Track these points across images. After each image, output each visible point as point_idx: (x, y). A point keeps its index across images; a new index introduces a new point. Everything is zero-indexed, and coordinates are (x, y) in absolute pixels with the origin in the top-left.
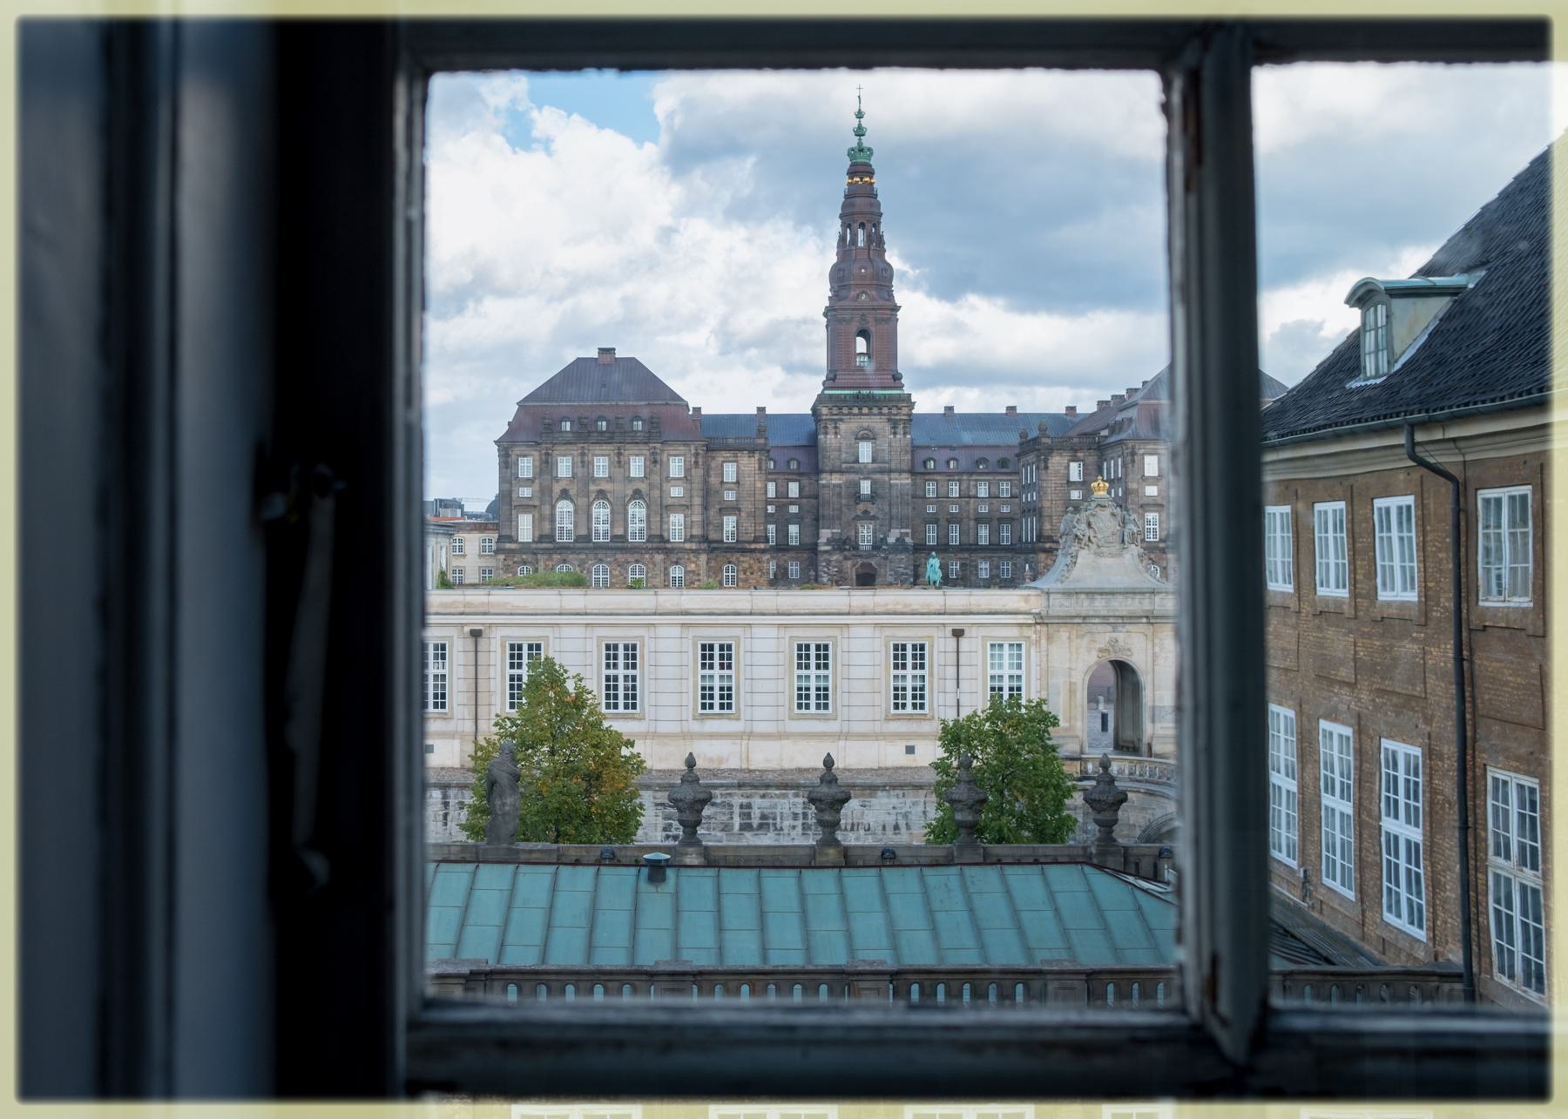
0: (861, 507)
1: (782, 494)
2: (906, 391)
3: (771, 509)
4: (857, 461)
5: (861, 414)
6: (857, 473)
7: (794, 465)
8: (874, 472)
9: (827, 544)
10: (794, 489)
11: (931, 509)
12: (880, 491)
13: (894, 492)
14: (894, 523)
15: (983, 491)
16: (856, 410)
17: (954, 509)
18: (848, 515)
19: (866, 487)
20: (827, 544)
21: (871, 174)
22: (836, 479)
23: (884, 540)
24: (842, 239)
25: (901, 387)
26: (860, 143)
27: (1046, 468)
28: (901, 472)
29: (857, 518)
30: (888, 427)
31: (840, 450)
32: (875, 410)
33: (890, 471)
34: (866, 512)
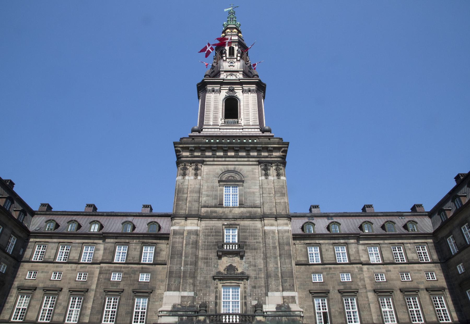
1: (134, 263)
3: (115, 277)
4: (220, 205)
6: (219, 218)
8: (242, 218)
11: (318, 278)
12: (251, 241)
13: (270, 241)
14: (273, 283)
17: (346, 278)
18: (205, 272)
19: (231, 236)
22: (192, 225)
23: (258, 308)
29: (219, 277)
30: (258, 170)
31: (199, 192)
33: (263, 217)
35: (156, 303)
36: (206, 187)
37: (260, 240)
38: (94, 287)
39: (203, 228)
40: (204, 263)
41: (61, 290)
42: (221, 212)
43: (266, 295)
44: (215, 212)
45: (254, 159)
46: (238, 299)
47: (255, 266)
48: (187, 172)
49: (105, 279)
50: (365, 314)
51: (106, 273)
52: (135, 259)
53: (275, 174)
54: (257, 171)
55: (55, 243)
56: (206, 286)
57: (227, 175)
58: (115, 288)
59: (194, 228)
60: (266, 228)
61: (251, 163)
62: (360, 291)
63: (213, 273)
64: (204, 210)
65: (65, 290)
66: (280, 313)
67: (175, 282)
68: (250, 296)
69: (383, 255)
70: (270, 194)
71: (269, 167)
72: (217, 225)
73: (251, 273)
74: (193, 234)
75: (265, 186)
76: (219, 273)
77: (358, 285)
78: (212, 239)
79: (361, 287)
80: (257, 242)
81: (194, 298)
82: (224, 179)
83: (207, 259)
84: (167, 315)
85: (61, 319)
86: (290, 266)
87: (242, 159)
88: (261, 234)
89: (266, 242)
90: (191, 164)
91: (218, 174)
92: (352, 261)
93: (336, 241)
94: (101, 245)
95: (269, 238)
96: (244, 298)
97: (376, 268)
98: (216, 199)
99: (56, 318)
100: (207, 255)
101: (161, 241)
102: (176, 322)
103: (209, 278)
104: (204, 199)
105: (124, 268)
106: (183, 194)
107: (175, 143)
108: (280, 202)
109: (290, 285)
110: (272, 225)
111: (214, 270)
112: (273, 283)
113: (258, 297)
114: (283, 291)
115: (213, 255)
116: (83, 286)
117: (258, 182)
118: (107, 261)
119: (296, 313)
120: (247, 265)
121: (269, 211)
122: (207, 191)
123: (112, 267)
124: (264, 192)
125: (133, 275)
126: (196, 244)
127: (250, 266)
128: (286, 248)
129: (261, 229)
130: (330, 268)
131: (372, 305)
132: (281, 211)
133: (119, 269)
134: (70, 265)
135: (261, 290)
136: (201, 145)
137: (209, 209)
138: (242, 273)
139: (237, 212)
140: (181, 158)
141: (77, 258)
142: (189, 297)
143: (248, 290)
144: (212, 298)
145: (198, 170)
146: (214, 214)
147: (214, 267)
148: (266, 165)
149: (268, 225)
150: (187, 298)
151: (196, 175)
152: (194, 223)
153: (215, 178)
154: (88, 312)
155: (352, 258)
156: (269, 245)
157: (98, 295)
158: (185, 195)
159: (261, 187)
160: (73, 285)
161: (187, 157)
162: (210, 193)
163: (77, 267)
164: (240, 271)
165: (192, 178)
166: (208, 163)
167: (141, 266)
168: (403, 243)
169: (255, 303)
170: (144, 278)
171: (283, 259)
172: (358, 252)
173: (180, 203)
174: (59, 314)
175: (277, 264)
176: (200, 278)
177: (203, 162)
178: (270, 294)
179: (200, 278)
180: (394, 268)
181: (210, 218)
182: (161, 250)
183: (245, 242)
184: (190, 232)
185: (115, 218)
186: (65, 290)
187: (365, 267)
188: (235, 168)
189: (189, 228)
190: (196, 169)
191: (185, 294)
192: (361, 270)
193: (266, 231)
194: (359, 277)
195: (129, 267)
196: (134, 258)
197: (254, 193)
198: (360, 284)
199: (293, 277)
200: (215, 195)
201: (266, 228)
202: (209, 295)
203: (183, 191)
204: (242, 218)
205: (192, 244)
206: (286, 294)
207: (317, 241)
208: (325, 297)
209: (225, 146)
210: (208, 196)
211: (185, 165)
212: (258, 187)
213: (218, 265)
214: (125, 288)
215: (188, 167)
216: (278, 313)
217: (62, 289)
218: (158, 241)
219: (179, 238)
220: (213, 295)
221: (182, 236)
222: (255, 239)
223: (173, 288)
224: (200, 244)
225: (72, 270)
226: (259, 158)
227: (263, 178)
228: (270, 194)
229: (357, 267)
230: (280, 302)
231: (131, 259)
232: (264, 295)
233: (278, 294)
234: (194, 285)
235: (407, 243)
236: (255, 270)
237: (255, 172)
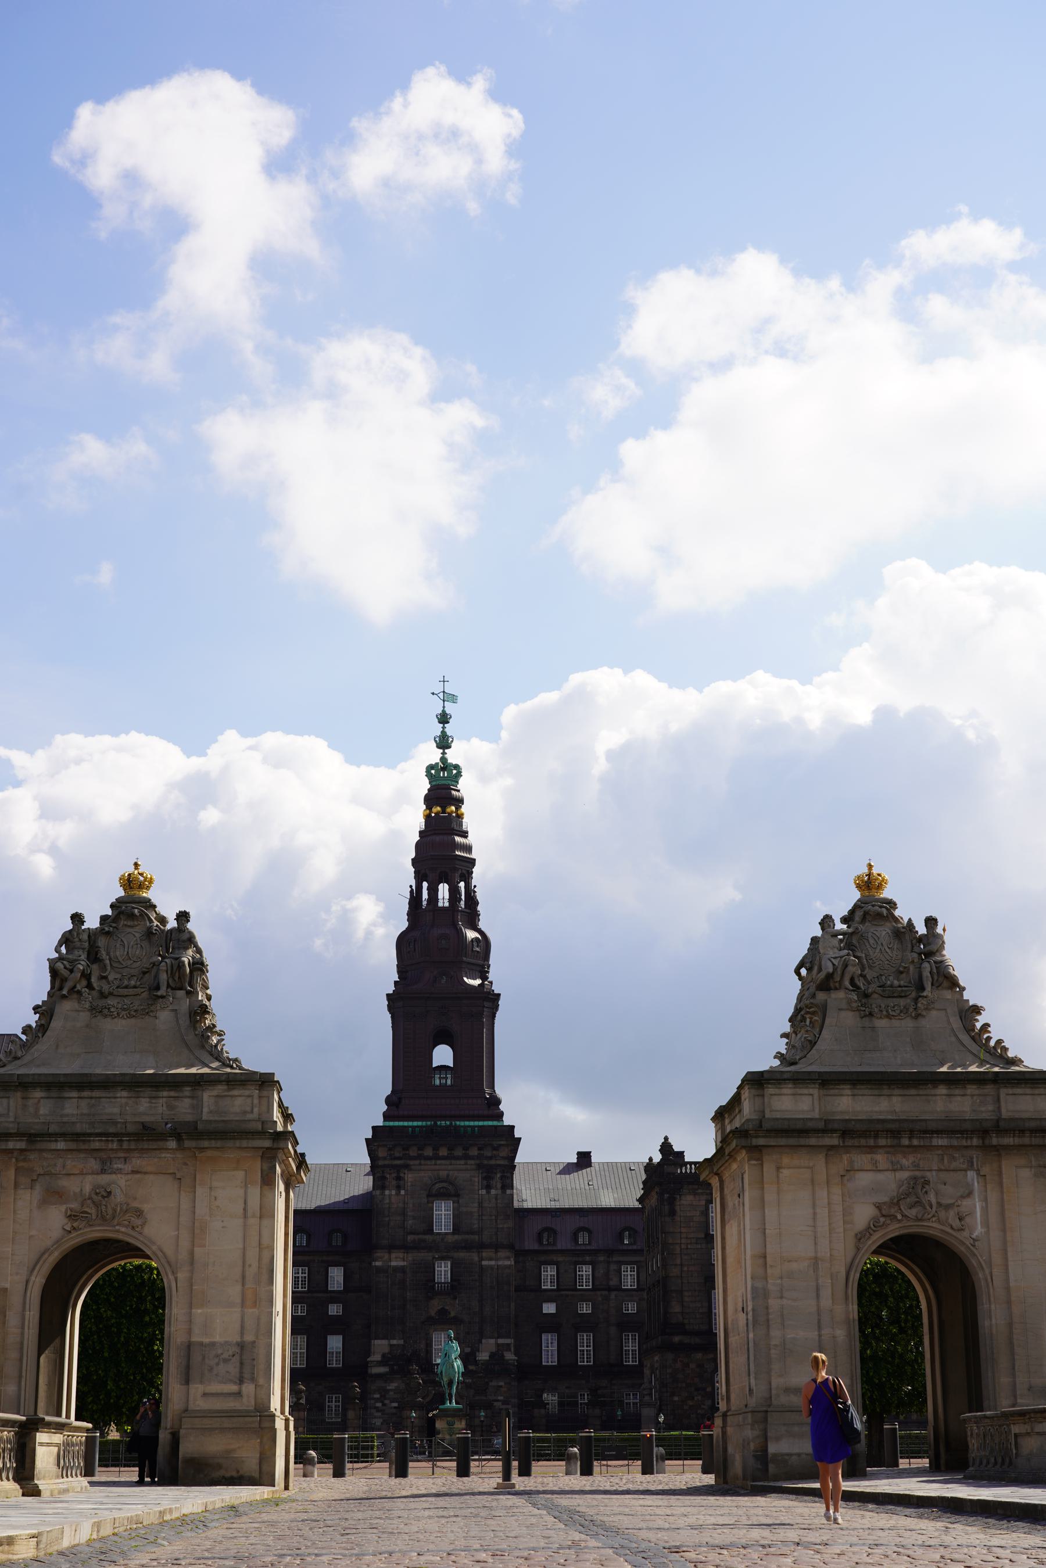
0: (436, 1305)
2: (507, 1121)
4: (430, 1230)
5: (436, 1157)
7: (337, 1240)
8: (457, 1247)
10: (336, 1277)
11: (549, 1308)
15: (629, 1278)
16: (429, 1152)
17: (585, 1309)
19: (443, 1271)
21: (459, 802)
22: (397, 1260)
24: (415, 899)
25: (501, 1115)
26: (443, 759)
27: (673, 1213)
28: (497, 1247)
32: (459, 1152)
33: (482, 1246)
45: (473, 1162)
53: (499, 1185)
54: (476, 1179)
59: (402, 1263)
60: (484, 1263)
61: (469, 1167)
64: (410, 1238)
75: (485, 1205)
87: (458, 1162)
104: (410, 1222)
107: (367, 1140)
110: (491, 1259)
130: (567, 1296)
137: (416, 1237)
144: (423, 1346)
151: (398, 1188)
159: (480, 1205)
161: (385, 1158)
164: (453, 1314)
165: (393, 1192)
170: (334, 1310)
177: (407, 1167)
184: (396, 1269)
187: (613, 1295)
188: (448, 1176)
189: (393, 1264)
190: (399, 1178)
191: (395, 1342)
201: (484, 1263)
206: (501, 1341)
207: (555, 1259)
212: (476, 1205)
227: (484, 1192)
230: (494, 1350)
233: (492, 1341)
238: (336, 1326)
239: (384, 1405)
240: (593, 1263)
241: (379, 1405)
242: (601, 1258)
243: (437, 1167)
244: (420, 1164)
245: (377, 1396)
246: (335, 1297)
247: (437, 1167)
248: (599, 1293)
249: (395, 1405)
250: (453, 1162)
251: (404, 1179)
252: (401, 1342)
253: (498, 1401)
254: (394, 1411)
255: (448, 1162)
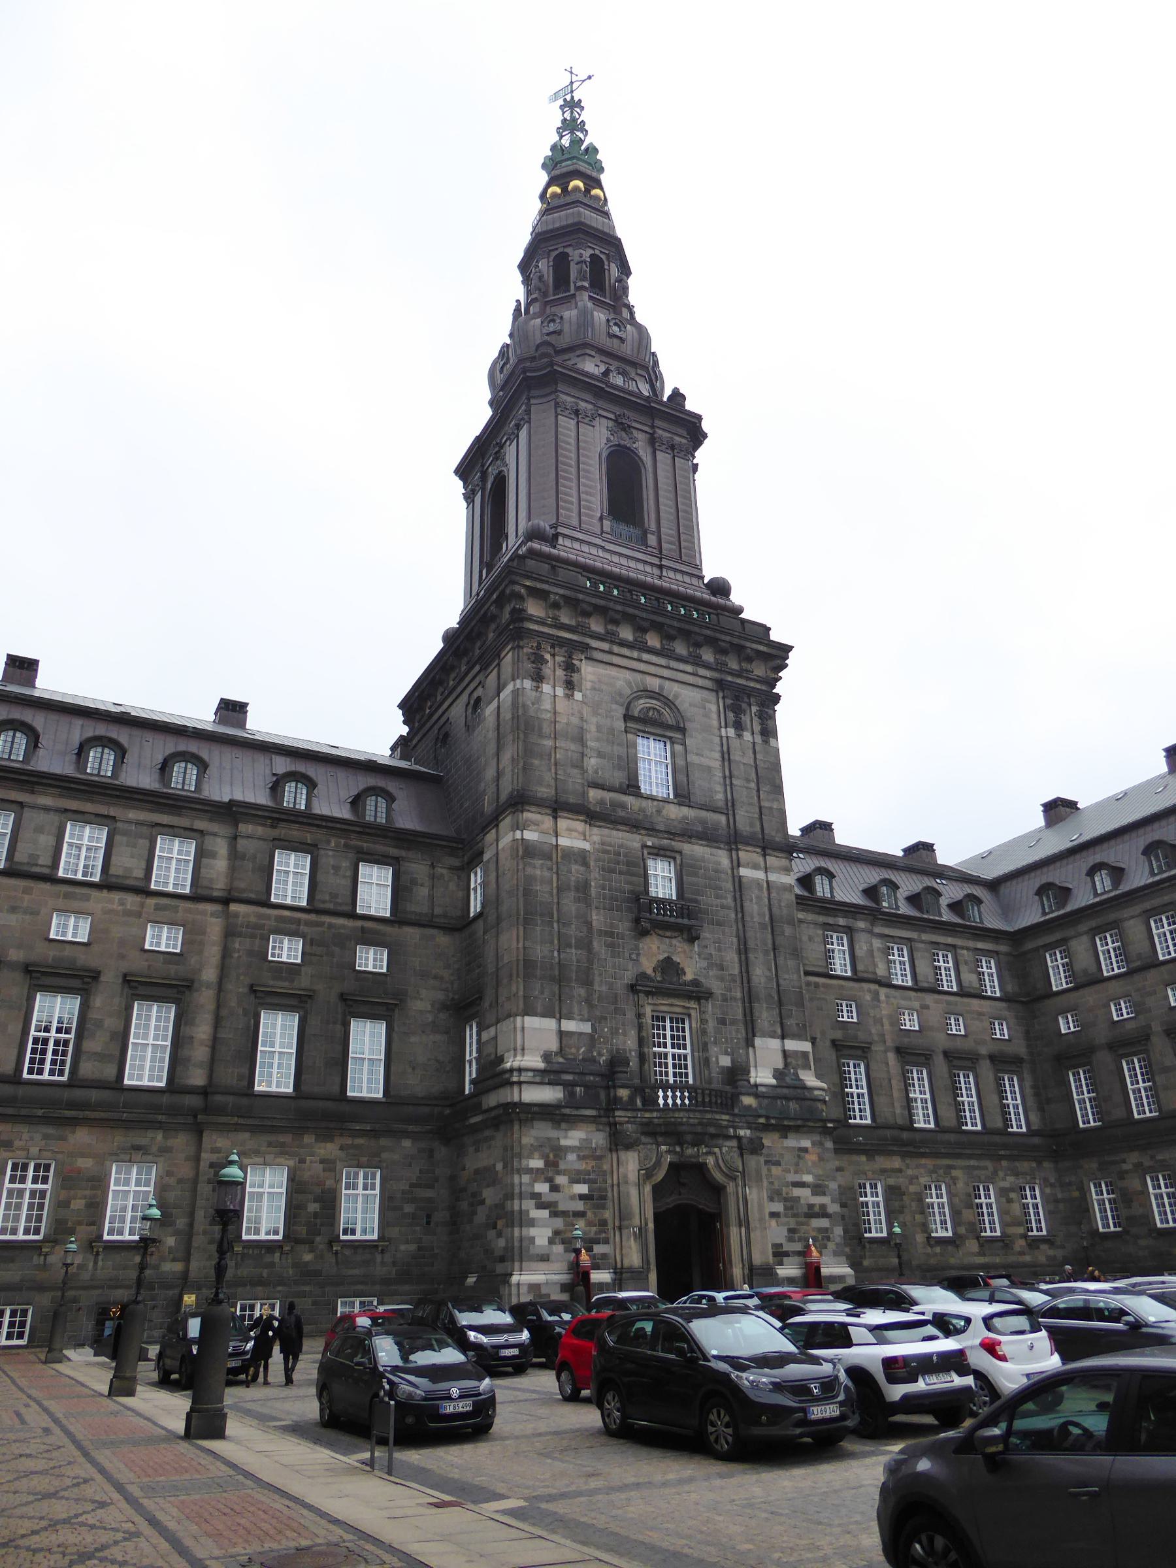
1: (330, 908)
3: (287, 950)
4: (632, 787)
6: (635, 825)
8: (688, 834)
9: (548, 1075)
10: (375, 891)
12: (708, 900)
13: (755, 908)
14: (765, 1016)
17: (848, 1014)
19: (662, 881)
20: (548, 1075)
22: (573, 836)
23: (737, 1074)
31: (580, 739)
34: (668, 966)
35: (413, 1039)
36: (593, 729)
37: (729, 901)
38: (209, 974)
39: (597, 846)
40: (607, 946)
41: (95, 975)
42: (636, 808)
43: (749, 1043)
44: (623, 806)
45: (707, 673)
46: (685, 1048)
47: (721, 967)
48: (547, 670)
49: (250, 953)
50: (881, 1101)
51: (253, 936)
52: (339, 901)
54: (714, 708)
55: (47, 809)
56: (616, 1009)
57: (642, 704)
58: (286, 984)
61: (700, 682)
62: (874, 1048)
63: (629, 976)
64: (594, 794)
65: (110, 978)
66: (785, 1091)
67: (542, 993)
68: (715, 1043)
69: (918, 970)
70: (748, 781)
71: (744, 706)
72: (629, 843)
73: (716, 987)
74: (576, 862)
75: (736, 756)
76: (643, 976)
77: (871, 1034)
78: (620, 882)
79: (876, 1038)
80: (723, 907)
81: (591, 1037)
82: (636, 713)
83: (611, 934)
84: (538, 1079)
85: (110, 1072)
86: (795, 977)
87: (682, 666)
88: (729, 886)
89: (745, 909)
90: (553, 646)
91: (620, 695)
92: (860, 975)
93: (831, 920)
94: (219, 840)
95: (751, 901)
96: (702, 1046)
97: (904, 999)
98: (619, 768)
99: (88, 1069)
100: (612, 926)
101: (411, 854)
102: (559, 1100)
103: (621, 991)
104: (592, 762)
105: (308, 923)
106: (541, 736)
108: (771, 808)
109: (798, 1025)
110: (755, 867)
111: (630, 967)
112: (765, 1015)
113: (732, 1048)
114: (783, 1037)
115: (624, 926)
116: (173, 969)
117: (717, 740)
118: (252, 896)
119: (816, 1093)
120: (704, 964)
121: (748, 828)
122: (598, 740)
123: (268, 917)
124: (735, 773)
125: (337, 950)
126: (583, 888)
127: (710, 966)
128: (788, 930)
129: (730, 872)
130: (817, 985)
131: (894, 1082)
132: (773, 833)
133: (294, 927)
134: (116, 896)
135: (737, 1031)
136: (581, 596)
137: (608, 796)
138: (696, 983)
139: (673, 816)
140: (522, 620)
141: (139, 873)
142: (581, 1034)
143: (711, 1025)
144: (630, 1043)
145: (573, 671)
146: (621, 813)
147: (631, 959)
148: (737, 698)
149: (747, 866)
150: (576, 1037)
152: (576, 831)
153: (614, 706)
154: (200, 1053)
155: (860, 967)
156: (752, 918)
157: (233, 1004)
158: (549, 743)
159: (726, 756)
160: (137, 964)
162: (607, 749)
163: (142, 905)
164: (689, 976)
165: (560, 691)
166: (598, 655)
167: (359, 923)
168: (954, 946)
169: (725, 1061)
170: (371, 960)
171: (782, 958)
172: (871, 952)
173: (536, 762)
174: (101, 1057)
175: (770, 970)
176: (600, 986)
177: (585, 648)
178: (758, 1041)
179: (600, 987)
180: (937, 1002)
181: (612, 822)
182: (414, 882)
183: (696, 901)
184: (571, 855)
185: (149, 735)
186: (110, 978)
187: (883, 991)
188: (661, 687)
189: (564, 842)
190: (570, 668)
191: (569, 1025)
192: (876, 996)
193: (744, 880)
194: (872, 1012)
195: (321, 924)
196: (336, 896)
197: (709, 769)
198: (873, 1031)
199: (803, 1005)
200: (619, 757)
201: (744, 872)
202: (625, 1034)
203: (540, 729)
204: (688, 834)
205: (577, 889)
206: (791, 1045)
208: (970, 1069)
209: (644, 615)
210: (600, 755)
211: (539, 648)
212: (717, 755)
213: (638, 955)
214: (315, 987)
215: (548, 657)
216: (779, 1090)
217: (99, 973)
218: (403, 853)
219: (542, 865)
220: (633, 1033)
221: (549, 863)
222: (717, 897)
223: (539, 1009)
224: (593, 892)
225: (127, 913)
226: (720, 671)
227: (731, 732)
228: (748, 781)
229: (869, 991)
231: (327, 898)
232: (743, 1043)
233: (775, 1043)
234: (588, 1001)
235: (962, 948)
236: (722, 979)
237: (710, 710)
238: (370, 998)
239: (555, 1188)
240: (849, 931)
241: (542, 1188)
242: (861, 925)
243: (642, 667)
244: (610, 652)
245: (537, 1163)
246: (371, 931)
247: (642, 667)
248: (865, 986)
249: (583, 1189)
250: (673, 664)
251: (579, 670)
252: (586, 1028)
253: (802, 1185)
254: (579, 1206)
255: (663, 661)
